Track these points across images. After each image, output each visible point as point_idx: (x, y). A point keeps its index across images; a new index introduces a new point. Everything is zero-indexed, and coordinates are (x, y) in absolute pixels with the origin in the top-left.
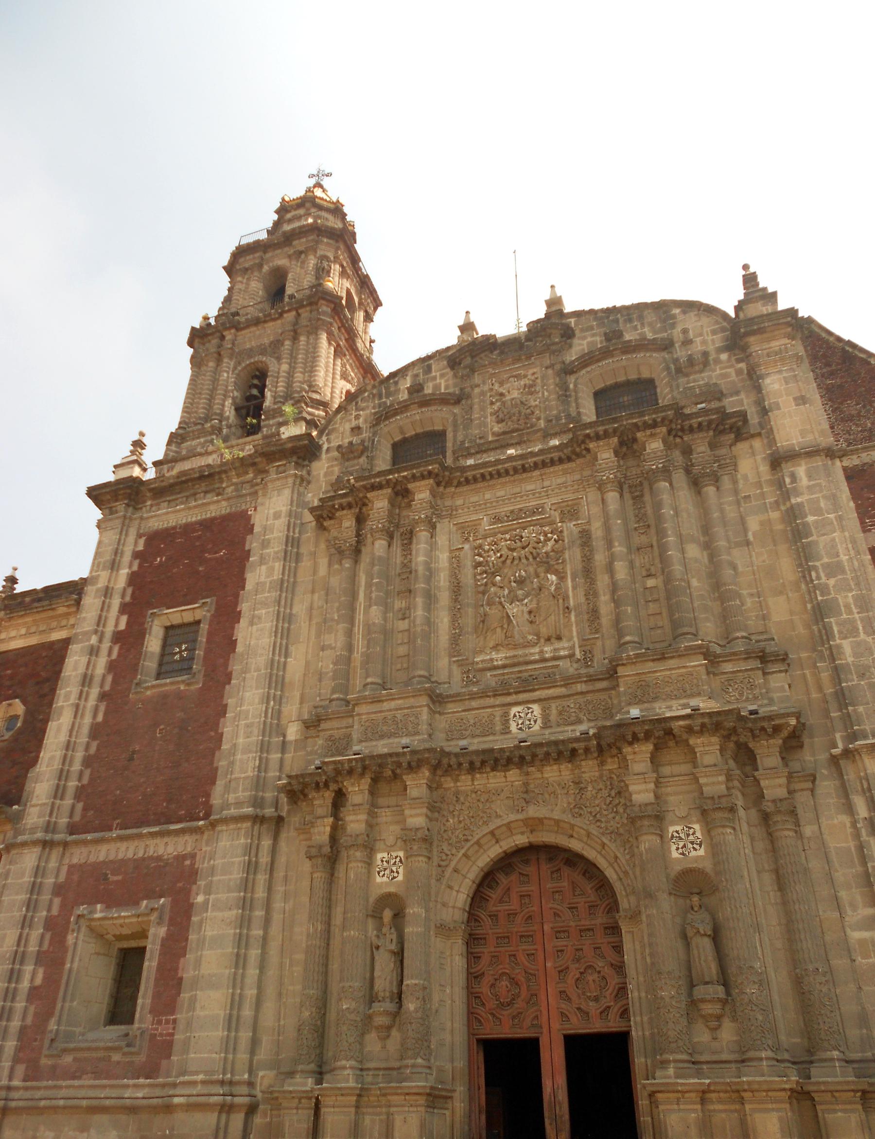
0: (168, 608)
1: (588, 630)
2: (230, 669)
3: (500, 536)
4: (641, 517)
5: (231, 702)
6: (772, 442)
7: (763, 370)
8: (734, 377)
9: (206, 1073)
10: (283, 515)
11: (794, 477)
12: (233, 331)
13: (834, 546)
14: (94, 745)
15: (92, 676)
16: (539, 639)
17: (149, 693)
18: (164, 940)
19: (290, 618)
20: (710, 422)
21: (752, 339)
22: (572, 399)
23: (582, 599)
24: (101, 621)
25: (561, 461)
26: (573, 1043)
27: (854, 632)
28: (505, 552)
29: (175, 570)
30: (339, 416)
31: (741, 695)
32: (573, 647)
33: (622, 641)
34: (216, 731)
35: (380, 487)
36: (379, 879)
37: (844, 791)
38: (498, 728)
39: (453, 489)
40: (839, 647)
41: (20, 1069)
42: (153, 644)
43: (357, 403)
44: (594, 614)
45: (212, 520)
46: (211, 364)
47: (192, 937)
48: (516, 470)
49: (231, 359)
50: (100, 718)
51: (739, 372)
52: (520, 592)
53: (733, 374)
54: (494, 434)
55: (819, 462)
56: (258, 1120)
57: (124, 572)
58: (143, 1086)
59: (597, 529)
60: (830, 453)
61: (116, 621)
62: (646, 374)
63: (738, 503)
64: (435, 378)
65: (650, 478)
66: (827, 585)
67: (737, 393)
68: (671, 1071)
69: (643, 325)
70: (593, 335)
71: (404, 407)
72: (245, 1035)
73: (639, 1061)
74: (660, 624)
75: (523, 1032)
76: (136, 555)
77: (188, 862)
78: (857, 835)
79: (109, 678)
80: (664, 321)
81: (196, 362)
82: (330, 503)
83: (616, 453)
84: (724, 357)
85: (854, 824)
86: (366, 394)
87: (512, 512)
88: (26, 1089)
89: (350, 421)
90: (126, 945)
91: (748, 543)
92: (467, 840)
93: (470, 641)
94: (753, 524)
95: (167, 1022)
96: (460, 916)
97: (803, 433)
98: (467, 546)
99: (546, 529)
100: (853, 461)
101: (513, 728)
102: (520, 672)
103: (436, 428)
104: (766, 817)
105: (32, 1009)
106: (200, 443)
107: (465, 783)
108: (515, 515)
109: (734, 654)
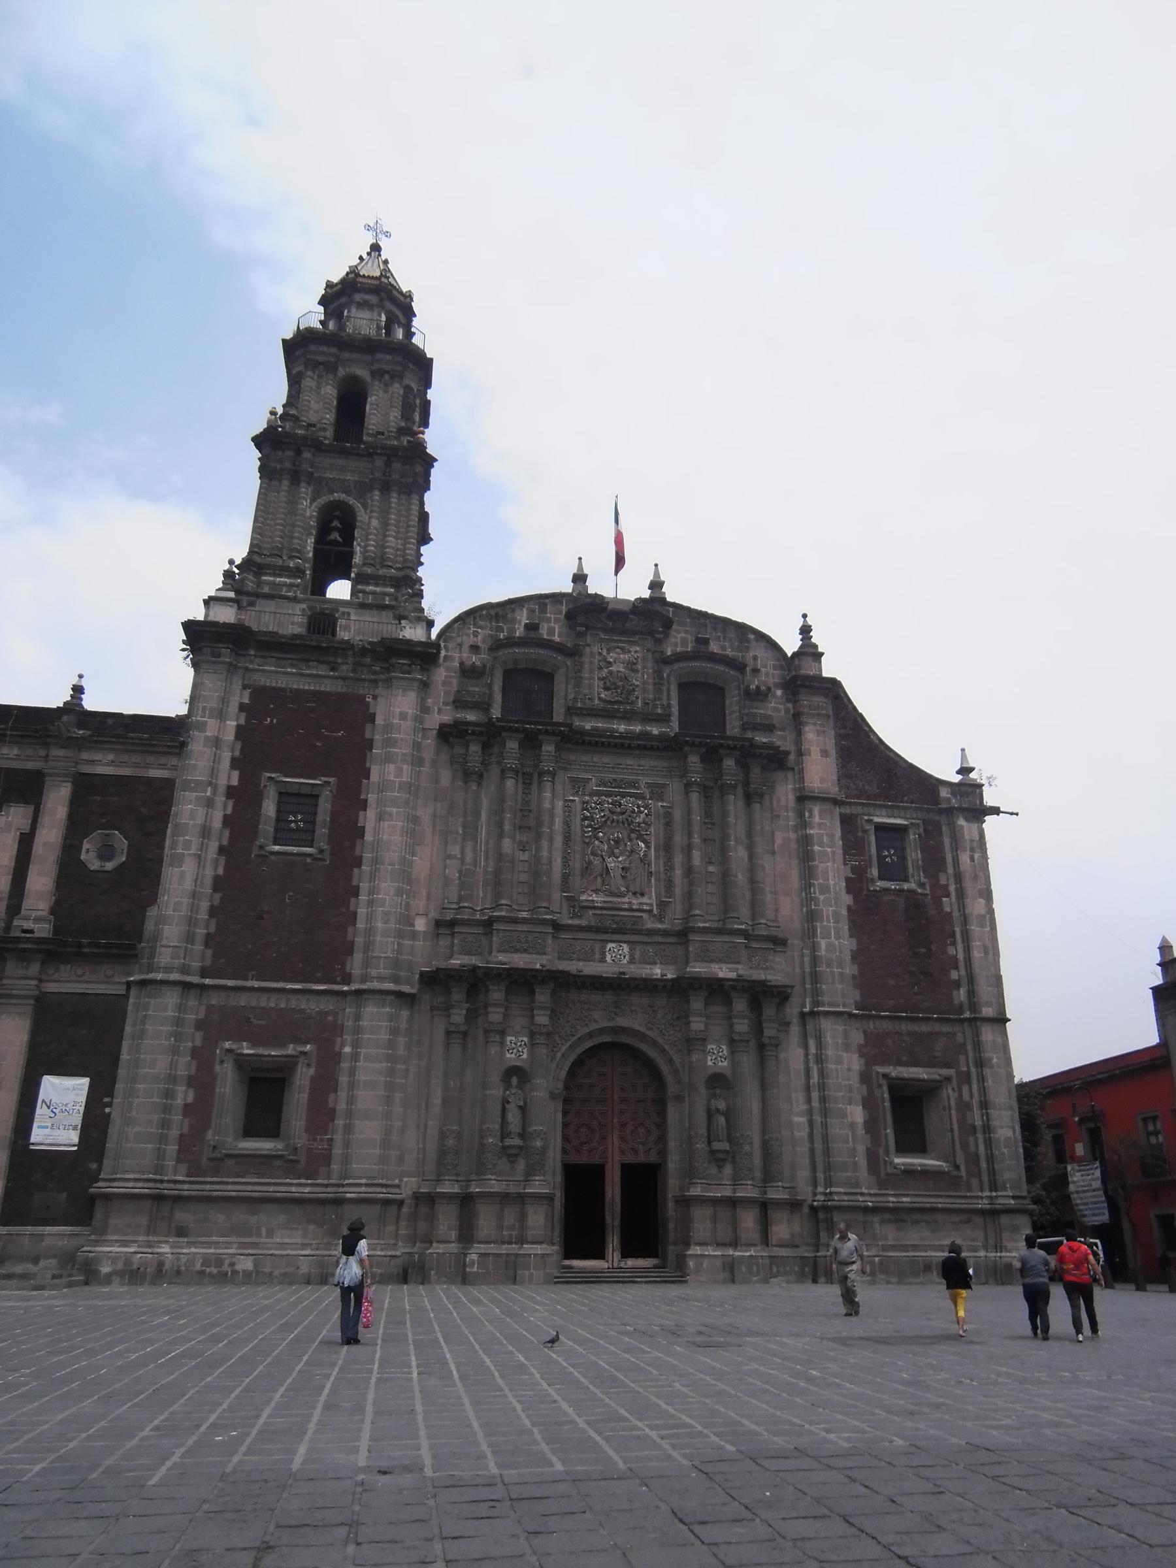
0: (286, 776)
1: (663, 893)
2: (357, 853)
3: (603, 797)
4: (708, 814)
5: (364, 886)
6: (802, 780)
7: (804, 719)
8: (782, 714)
9: (368, 1178)
11: (811, 811)
13: (827, 872)
14: (218, 896)
15: (210, 829)
16: (628, 892)
17: (273, 857)
18: (313, 1079)
19: (415, 820)
20: (768, 754)
22: (665, 688)
24: (213, 773)
25: (658, 749)
26: (628, 1170)
27: (828, 936)
28: (607, 813)
29: (288, 737)
30: (456, 625)
31: (759, 965)
32: (651, 905)
33: (692, 913)
34: (348, 908)
35: (517, 730)
36: (508, 1055)
37: (805, 1035)
38: (597, 956)
39: (570, 746)
40: (819, 943)
41: (183, 1168)
42: (269, 808)
43: (475, 619)
44: (669, 885)
45: (328, 695)
47: (344, 1079)
49: (309, 484)
50: (221, 871)
51: (787, 711)
52: (616, 851)
53: (783, 710)
54: (600, 699)
55: (827, 806)
57: (232, 724)
58: (306, 1185)
59: (677, 815)
60: (836, 802)
61: (229, 777)
62: (719, 684)
63: (772, 820)
64: (549, 620)
65: (724, 790)
66: (819, 899)
68: (699, 1189)
69: (724, 638)
70: (686, 632)
72: (393, 1153)
74: (714, 902)
76: (242, 707)
77: (330, 1018)
78: (807, 1062)
79: (227, 833)
80: (741, 642)
81: (265, 471)
82: (465, 728)
83: (703, 760)
84: (779, 692)
85: (807, 1055)
87: (614, 780)
88: (191, 1183)
89: (468, 635)
91: (773, 853)
92: (573, 1035)
93: (576, 881)
94: (779, 838)
95: (322, 1140)
96: (561, 1086)
97: (822, 780)
100: (847, 810)
101: (608, 959)
102: (614, 915)
103: (545, 669)
104: (761, 1047)
105: (187, 1121)
106: (285, 584)
109: (761, 936)
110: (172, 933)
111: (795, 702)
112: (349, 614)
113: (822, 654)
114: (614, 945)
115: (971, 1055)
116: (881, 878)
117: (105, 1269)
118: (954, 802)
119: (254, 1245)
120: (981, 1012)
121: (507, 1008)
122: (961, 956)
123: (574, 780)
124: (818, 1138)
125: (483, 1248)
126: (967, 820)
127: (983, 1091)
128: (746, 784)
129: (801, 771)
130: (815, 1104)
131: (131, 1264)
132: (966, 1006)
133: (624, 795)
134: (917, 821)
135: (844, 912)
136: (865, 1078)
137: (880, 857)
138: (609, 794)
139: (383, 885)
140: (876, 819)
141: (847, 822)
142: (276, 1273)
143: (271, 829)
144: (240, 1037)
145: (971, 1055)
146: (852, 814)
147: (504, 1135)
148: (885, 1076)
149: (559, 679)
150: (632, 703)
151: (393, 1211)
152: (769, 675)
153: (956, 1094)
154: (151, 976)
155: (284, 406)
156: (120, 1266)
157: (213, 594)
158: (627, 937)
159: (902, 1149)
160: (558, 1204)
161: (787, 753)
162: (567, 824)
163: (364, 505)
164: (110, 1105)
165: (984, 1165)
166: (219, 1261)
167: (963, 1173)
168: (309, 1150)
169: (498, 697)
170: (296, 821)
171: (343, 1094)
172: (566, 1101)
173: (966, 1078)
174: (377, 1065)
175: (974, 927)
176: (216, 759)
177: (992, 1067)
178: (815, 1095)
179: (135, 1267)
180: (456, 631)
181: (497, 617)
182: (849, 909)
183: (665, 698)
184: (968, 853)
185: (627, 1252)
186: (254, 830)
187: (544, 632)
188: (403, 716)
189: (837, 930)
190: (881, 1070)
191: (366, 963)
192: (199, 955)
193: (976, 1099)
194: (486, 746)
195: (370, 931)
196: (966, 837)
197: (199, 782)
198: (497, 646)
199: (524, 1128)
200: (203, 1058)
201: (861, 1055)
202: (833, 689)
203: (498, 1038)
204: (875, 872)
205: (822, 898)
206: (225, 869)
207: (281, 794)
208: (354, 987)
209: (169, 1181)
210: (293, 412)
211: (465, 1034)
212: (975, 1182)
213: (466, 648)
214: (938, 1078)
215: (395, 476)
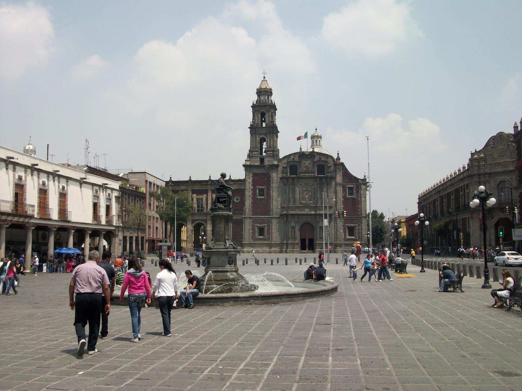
6: (336, 181)
61: (252, 187)
67: (333, 172)
71: (292, 162)
73: (315, 241)
75: (304, 238)
76: (252, 176)
81: (251, 133)
97: (339, 181)
107: (301, 216)
108: (306, 184)
110: (247, 210)
117: (245, 252)
118: (361, 183)
123: (300, 184)
126: (363, 185)
127: (361, 227)
136: (344, 226)
140: (348, 186)
141: (343, 187)
143: (258, 194)
144: (257, 224)
149: (298, 167)
151: (278, 245)
152: (331, 163)
155: (253, 120)
157: (246, 159)
159: (349, 236)
160: (300, 244)
162: (299, 191)
163: (267, 137)
166: (258, 251)
169: (289, 171)
170: (261, 193)
171: (271, 230)
172: (300, 230)
173: (359, 225)
175: (362, 203)
176: (250, 185)
181: (288, 157)
182: (343, 201)
185: (309, 250)
186: (256, 195)
187: (295, 159)
188: (275, 176)
191: (272, 213)
192: (251, 213)
194: (287, 180)
195: (272, 209)
198: (288, 162)
202: (342, 164)
204: (347, 195)
210: (254, 121)
211: (286, 222)
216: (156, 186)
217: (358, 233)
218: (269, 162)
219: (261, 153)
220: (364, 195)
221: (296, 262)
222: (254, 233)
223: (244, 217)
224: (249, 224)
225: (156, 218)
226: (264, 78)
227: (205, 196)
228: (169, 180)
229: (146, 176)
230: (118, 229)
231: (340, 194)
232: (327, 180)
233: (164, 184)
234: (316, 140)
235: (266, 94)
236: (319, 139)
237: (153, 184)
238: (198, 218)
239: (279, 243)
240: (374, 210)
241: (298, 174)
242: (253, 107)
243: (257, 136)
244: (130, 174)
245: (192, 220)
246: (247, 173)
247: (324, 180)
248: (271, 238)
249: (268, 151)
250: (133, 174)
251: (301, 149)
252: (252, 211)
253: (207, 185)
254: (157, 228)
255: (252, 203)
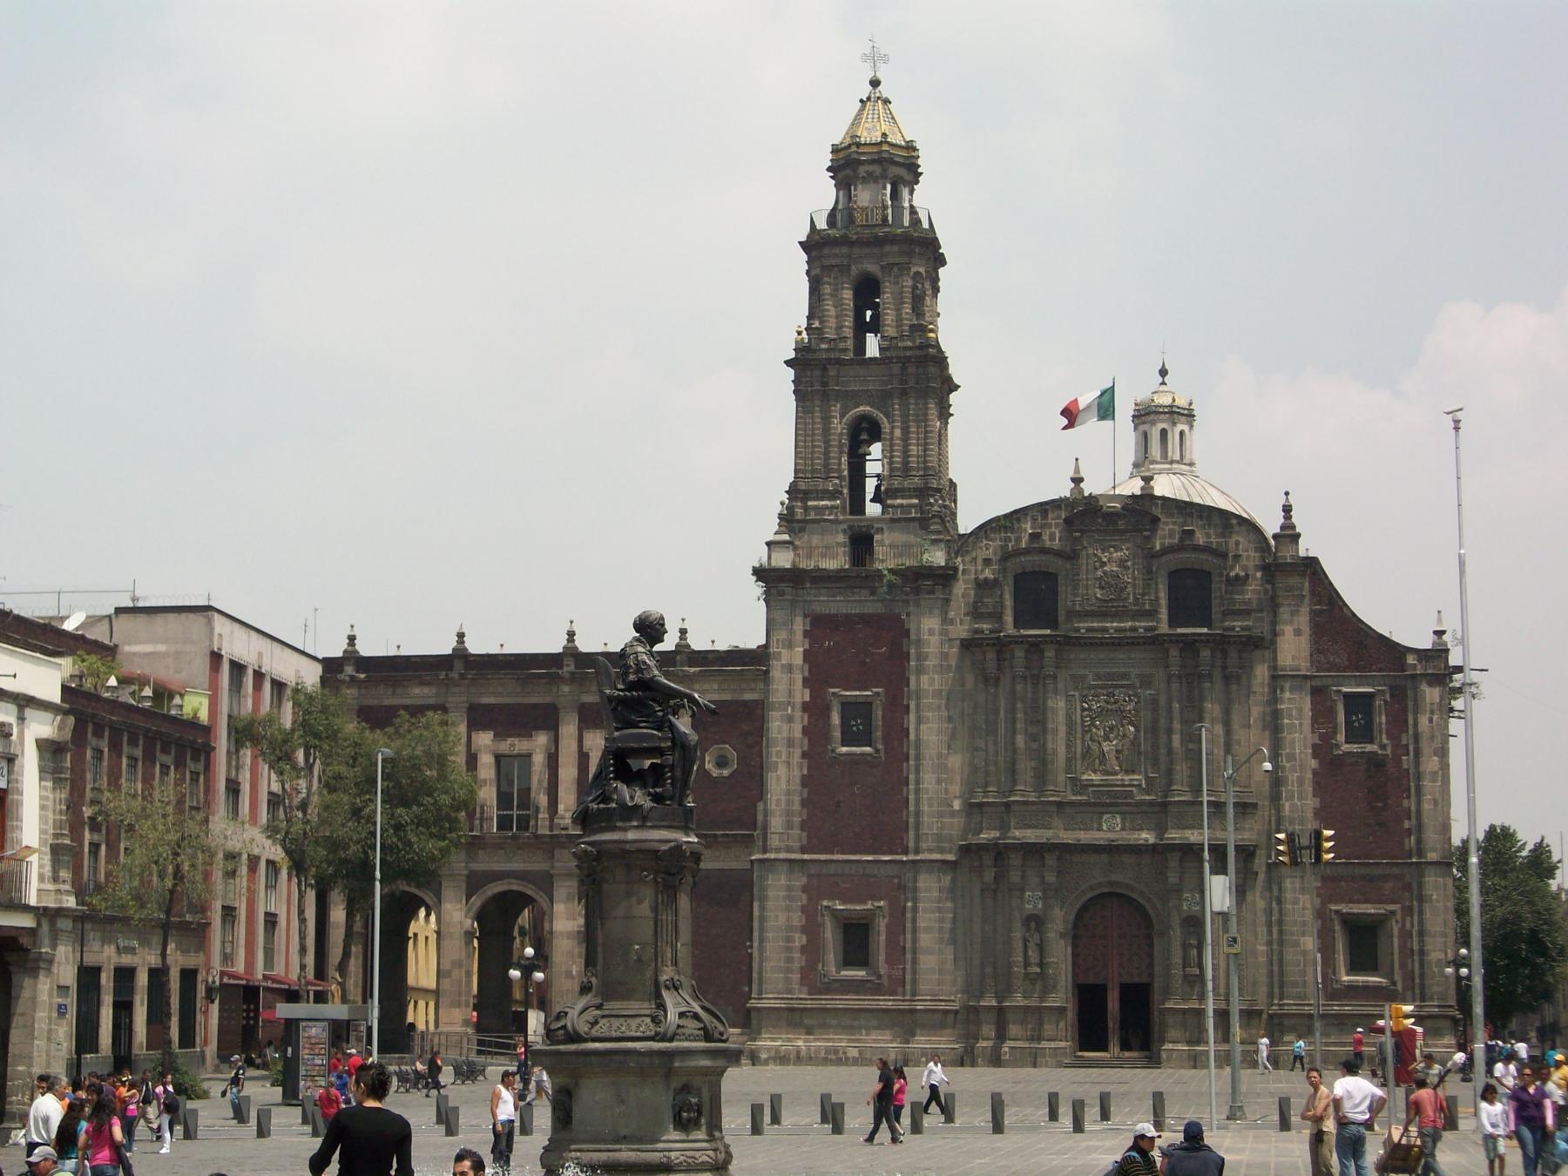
6: (1275, 659)
7: (1280, 600)
9: (931, 995)
10: (936, 632)
12: (837, 366)
13: (1294, 742)
14: (805, 792)
21: (1278, 573)
23: (1149, 749)
24: (790, 693)
25: (1144, 643)
28: (1103, 704)
40: (1283, 805)
41: (805, 989)
43: (986, 532)
46: (818, 402)
48: (1113, 644)
50: (805, 772)
56: (959, 1016)
58: (890, 1000)
59: (1163, 700)
61: (802, 695)
66: (1285, 767)
67: (1261, 611)
70: (1174, 523)
71: (1027, 551)
73: (1156, 997)
76: (806, 634)
79: (806, 741)
81: (802, 394)
86: (994, 525)
90: (848, 922)
91: (1249, 726)
96: (1070, 926)
97: (1294, 658)
98: (1077, 694)
99: (1131, 692)
101: (1105, 828)
105: (804, 958)
106: (826, 507)
108: (1110, 676)
110: (776, 823)
111: (1273, 584)
112: (882, 529)
113: (1299, 535)
114: (1109, 816)
115: (1415, 892)
116: (1346, 743)
117: (764, 1056)
119: (858, 1041)
120: (1425, 857)
121: (1024, 871)
122: (1413, 808)
124: (1275, 962)
125: (1012, 1044)
126: (1431, 684)
127: (1421, 922)
128: (1224, 668)
129: (1275, 651)
130: (1275, 936)
131: (780, 1053)
132: (1414, 852)
133: (1117, 687)
134: (1384, 688)
135: (1309, 775)
136: (1321, 914)
137: (1348, 723)
138: (1106, 687)
139: (926, 776)
140: (1345, 690)
141: (1319, 693)
142: (874, 1059)
143: (837, 734)
144: (832, 897)
145: (1415, 892)
146: (1323, 686)
147: (1027, 964)
148: (1337, 912)
149: (1061, 580)
150: (1125, 599)
151: (950, 1018)
152: (1248, 559)
153: (1400, 925)
154: (767, 856)
155: (809, 318)
156: (773, 1054)
157: (771, 538)
158: (1118, 809)
159: (1354, 968)
160: (1071, 1015)
161: (1262, 639)
163: (887, 415)
164: (751, 947)
165: (1417, 981)
166: (836, 1051)
167: (1399, 987)
168: (890, 976)
169: (1009, 602)
170: (857, 725)
171: (909, 936)
173: (1408, 911)
174: (932, 915)
176: (791, 682)
177: (1431, 901)
178: (1275, 929)
179: (782, 1054)
180: (971, 545)
181: (1006, 528)
182: (1315, 773)
183: (1153, 591)
184: (1428, 715)
185: (1125, 1046)
187: (1046, 538)
188: (931, 632)
189: (1300, 793)
190: (1334, 907)
191: (917, 839)
193: (1416, 928)
194: (999, 653)
195: (918, 813)
196: (1428, 701)
197: (781, 703)
198: (1006, 557)
199: (1041, 960)
200: (809, 912)
201: (1319, 895)
202: (1311, 566)
203: (1018, 893)
204: (1341, 737)
205: (1288, 765)
206: (809, 768)
207: (843, 704)
208: (911, 857)
209: (797, 999)
210: (816, 324)
211: (995, 891)
212: (1409, 994)
213: (979, 561)
214: (1383, 911)
215: (911, 383)
216: (267, 686)
217: (1407, 952)
218: (901, 555)
219: (857, 506)
220: (1432, 738)
221: (1053, 1116)
222: (813, 950)
223: (761, 861)
224: (790, 898)
225: (269, 862)
226: (875, 83)
227: (542, 739)
228: (340, 654)
229: (212, 630)
230: (52, 924)
231: (1300, 735)
232: (1225, 653)
233: (311, 676)
234: (1164, 433)
235: (884, 177)
236: (1180, 427)
237: (250, 672)
238: (497, 867)
239: (956, 1006)
240: (1498, 823)
241: (1061, 617)
242: (814, 245)
243: (836, 409)
244: (123, 617)
245: (468, 877)
246: (779, 615)
247: (1205, 654)
248: (908, 977)
249: (897, 490)
250: (141, 619)
251: (1077, 481)
252: (803, 826)
253: (554, 679)
254: (271, 920)
255: (804, 785)
